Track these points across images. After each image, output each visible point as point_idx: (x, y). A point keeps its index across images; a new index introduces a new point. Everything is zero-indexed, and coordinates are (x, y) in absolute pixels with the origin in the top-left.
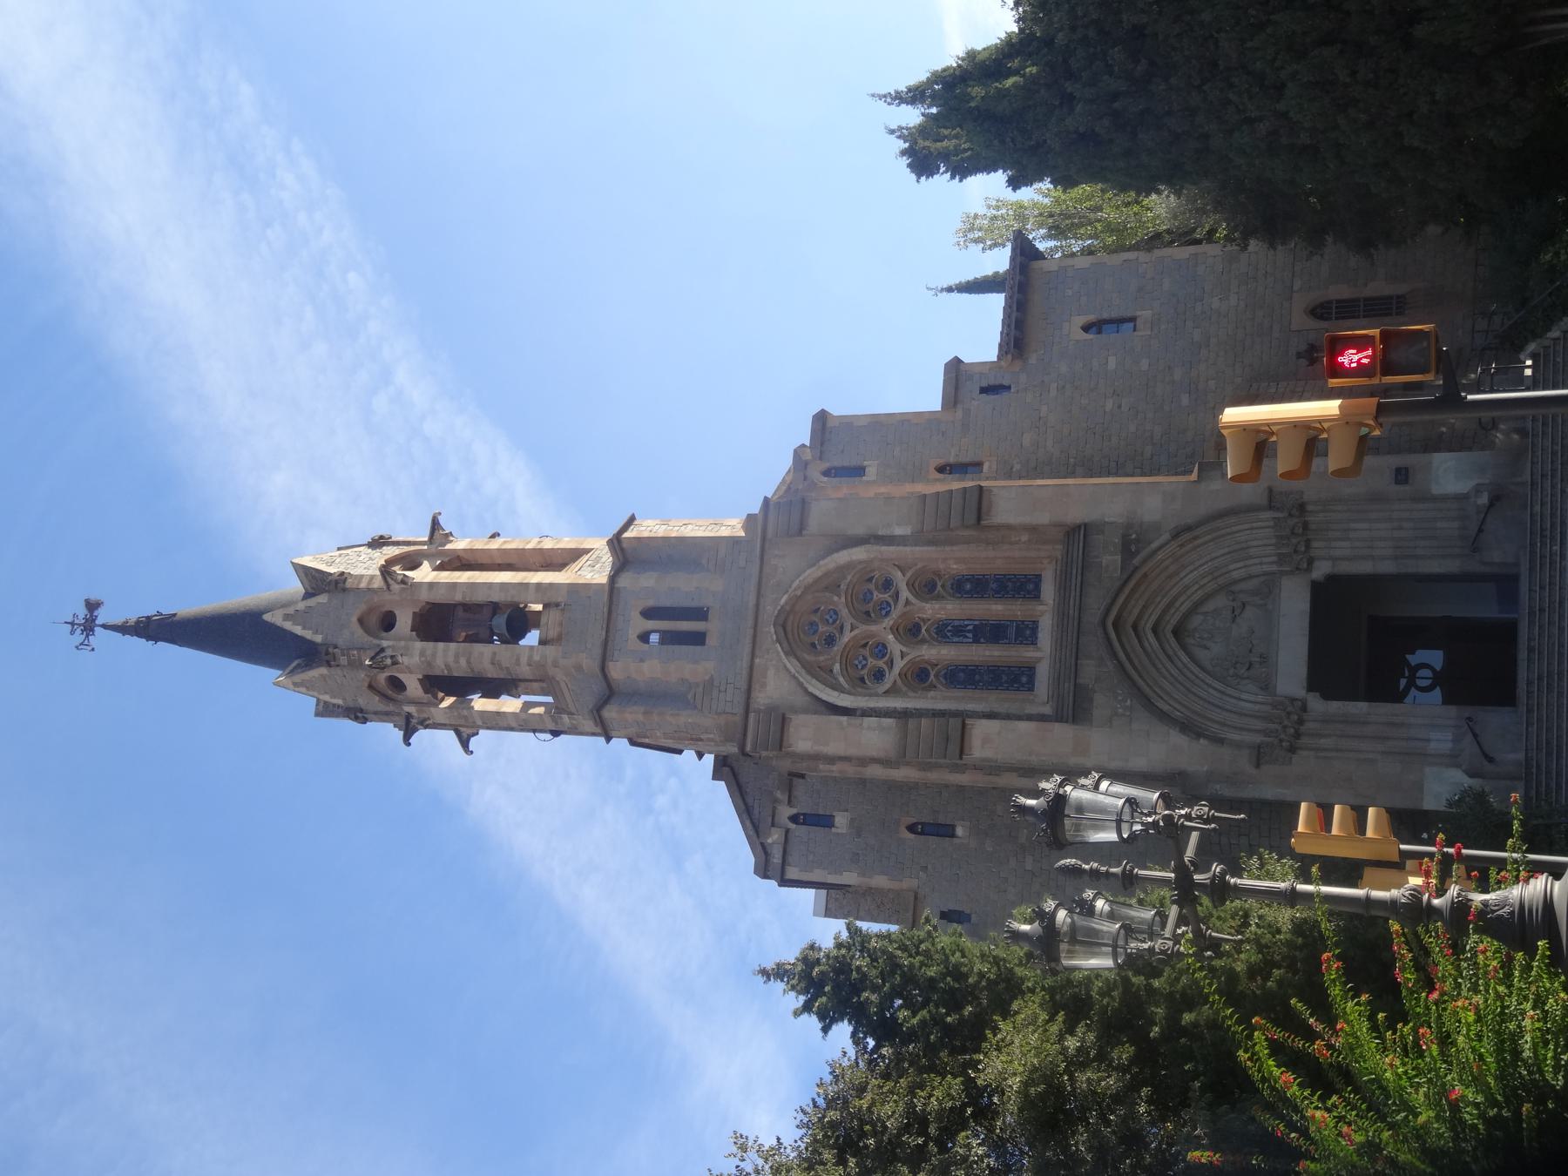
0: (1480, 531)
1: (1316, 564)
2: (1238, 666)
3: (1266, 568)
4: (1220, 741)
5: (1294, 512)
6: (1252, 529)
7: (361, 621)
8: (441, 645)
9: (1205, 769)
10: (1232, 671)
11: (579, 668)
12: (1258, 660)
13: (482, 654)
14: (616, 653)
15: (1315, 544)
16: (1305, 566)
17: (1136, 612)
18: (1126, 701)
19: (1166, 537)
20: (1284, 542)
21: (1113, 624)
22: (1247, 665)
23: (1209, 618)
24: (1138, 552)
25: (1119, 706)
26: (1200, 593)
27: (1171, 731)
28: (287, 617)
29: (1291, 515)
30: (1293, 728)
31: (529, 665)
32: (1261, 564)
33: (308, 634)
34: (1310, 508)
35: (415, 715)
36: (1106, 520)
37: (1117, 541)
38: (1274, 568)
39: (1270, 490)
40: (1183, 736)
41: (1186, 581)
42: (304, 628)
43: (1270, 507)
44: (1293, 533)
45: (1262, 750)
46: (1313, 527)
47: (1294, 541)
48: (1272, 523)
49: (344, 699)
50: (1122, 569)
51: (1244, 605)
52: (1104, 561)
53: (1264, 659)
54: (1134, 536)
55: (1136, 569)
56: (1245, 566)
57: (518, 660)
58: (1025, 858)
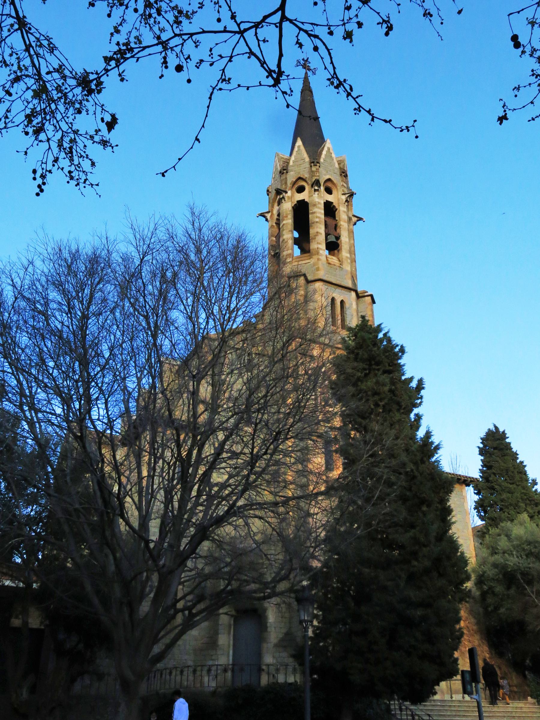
7: (329, 180)
8: (323, 212)
11: (318, 269)
13: (320, 228)
14: (327, 287)
28: (329, 149)
31: (318, 248)
33: (323, 156)
35: (287, 195)
42: (326, 155)
49: (292, 166)
57: (320, 244)
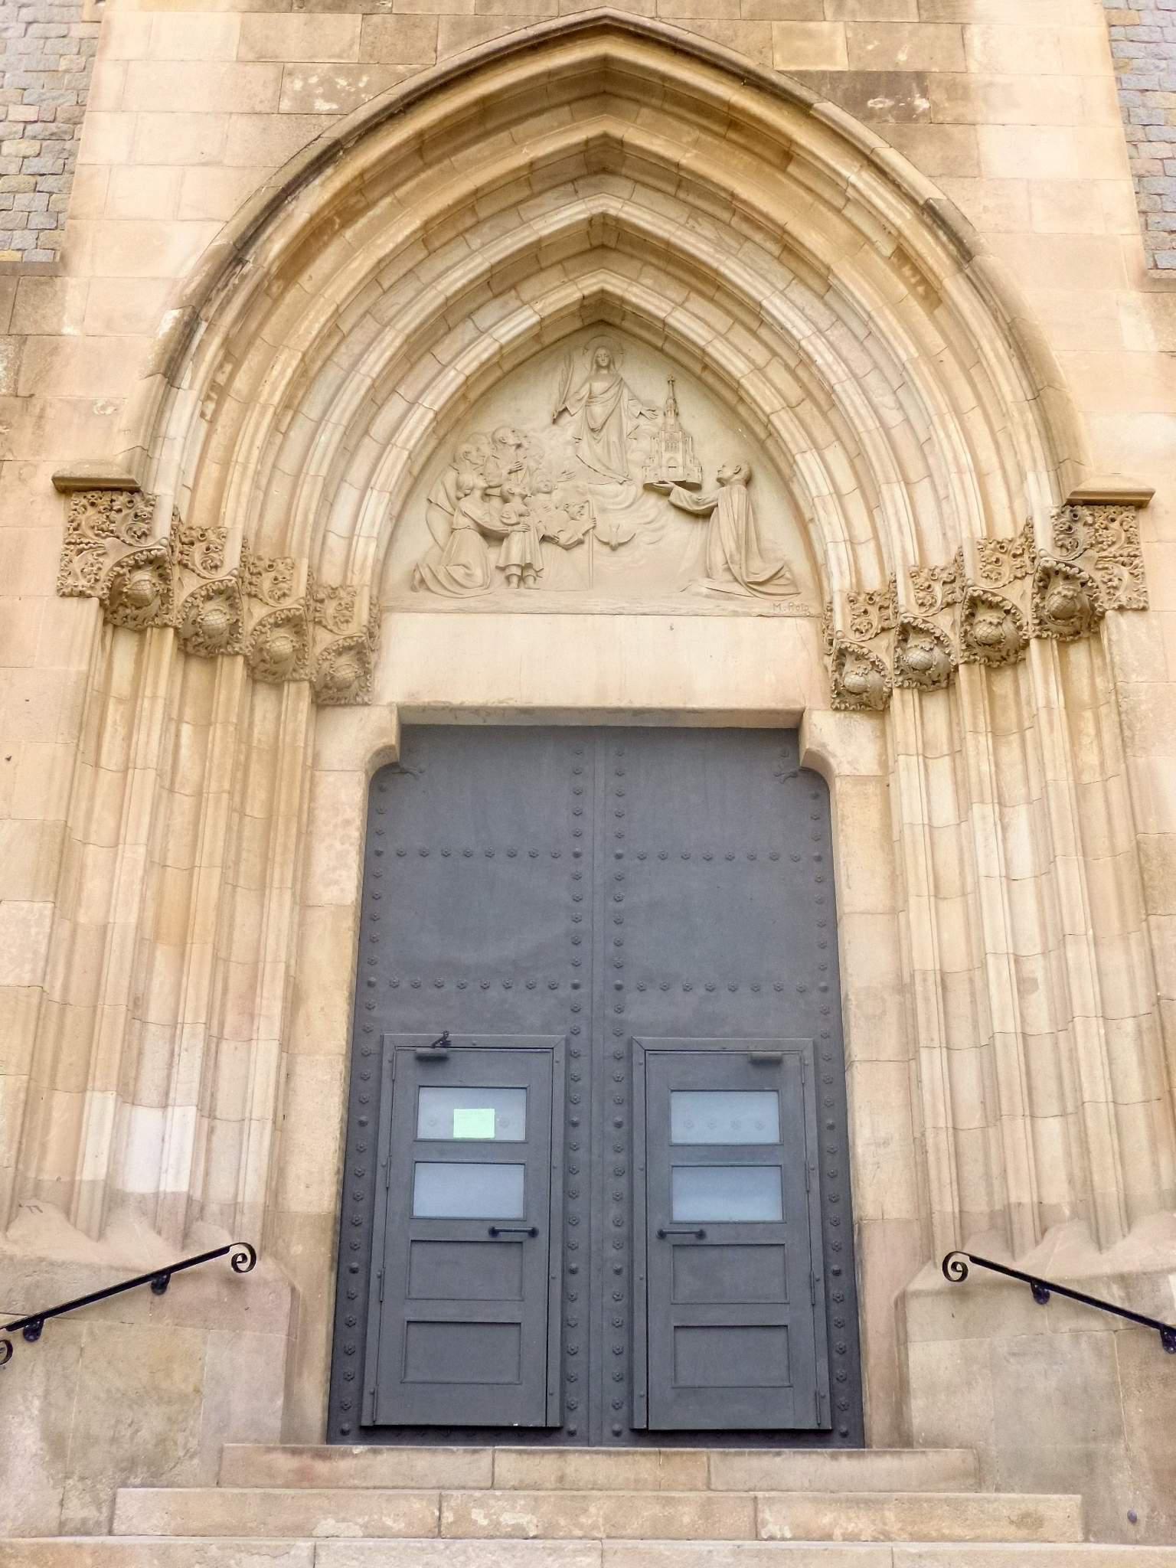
0: (1041, 1290)
1: (863, 727)
2: (496, 502)
3: (837, 558)
4: (170, 370)
5: (1059, 594)
6: (981, 477)
9: (67, 330)
10: (470, 478)
12: (515, 558)
15: (936, 707)
16: (853, 677)
17: (657, 145)
18: (327, 98)
19: (928, 190)
20: (938, 589)
21: (605, 60)
22: (496, 525)
23: (660, 420)
24: (868, 116)
25: (314, 80)
26: (737, 366)
27: (218, 226)
29: (1047, 577)
30: (234, 626)
32: (852, 542)
34: (1079, 654)
36: (974, 33)
37: (902, 57)
38: (839, 583)
39: (1139, 503)
40: (192, 262)
41: (777, 307)
43: (1078, 504)
44: (975, 604)
45: (121, 500)
46: (1004, 684)
47: (945, 623)
48: (1006, 530)
50: (803, 76)
51: (704, 515)
52: (825, 26)
53: (525, 573)
54: (921, 104)
55: (802, 108)
56: (839, 496)
58: (34, 138)
